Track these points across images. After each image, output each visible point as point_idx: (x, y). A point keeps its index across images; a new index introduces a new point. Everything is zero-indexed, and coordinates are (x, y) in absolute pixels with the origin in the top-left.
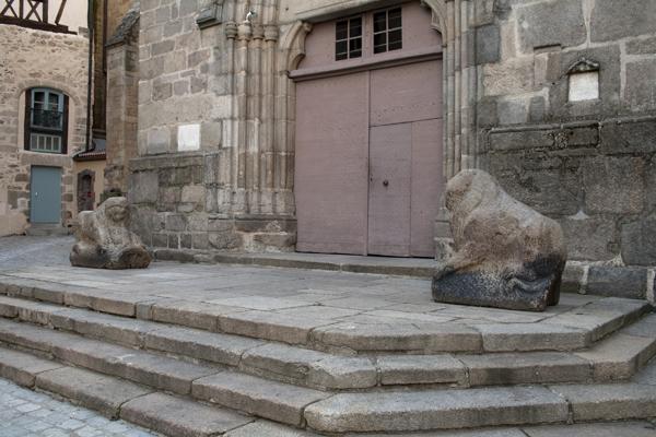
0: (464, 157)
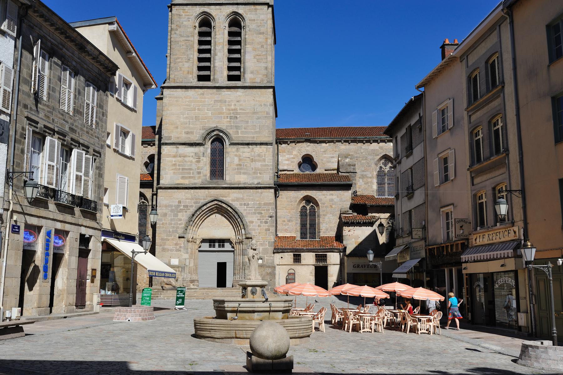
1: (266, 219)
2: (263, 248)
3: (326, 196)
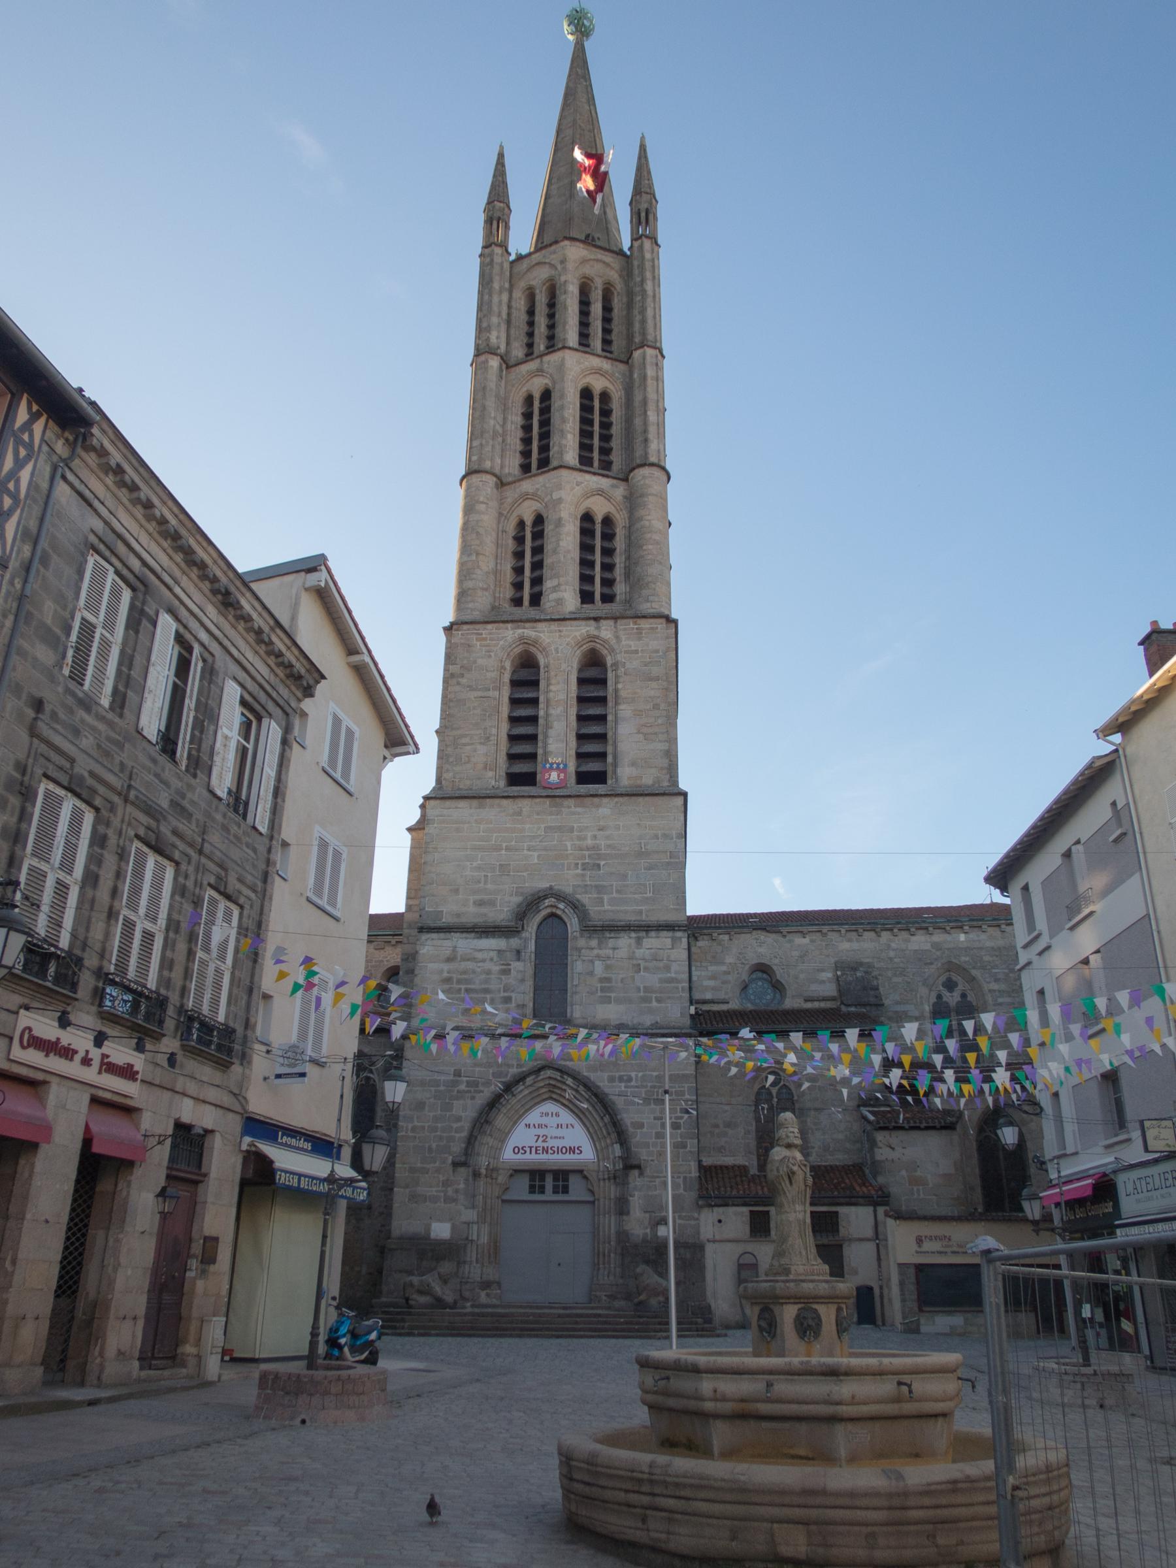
0: (612, 1255)
1: (677, 1118)
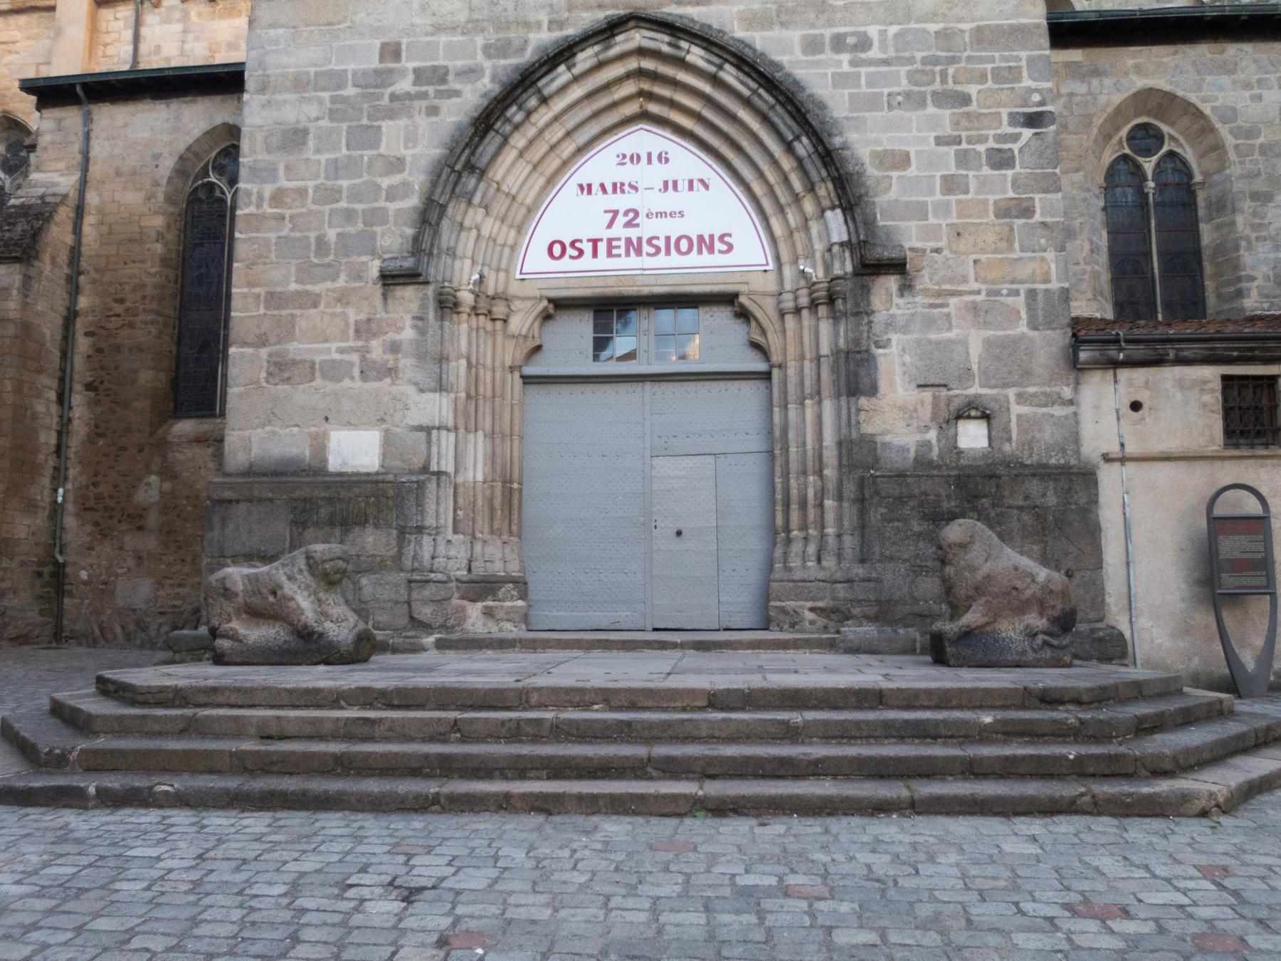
0: (829, 503)
2: (988, 343)
3: (1256, 91)
